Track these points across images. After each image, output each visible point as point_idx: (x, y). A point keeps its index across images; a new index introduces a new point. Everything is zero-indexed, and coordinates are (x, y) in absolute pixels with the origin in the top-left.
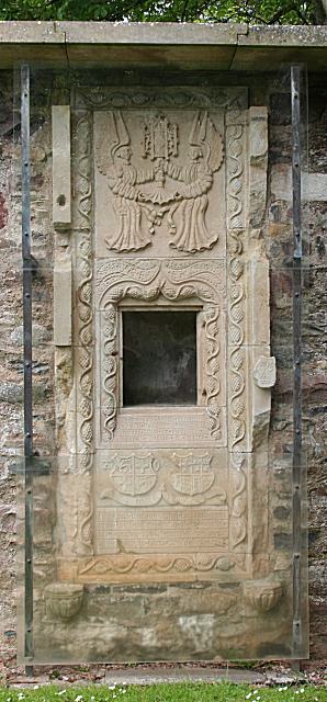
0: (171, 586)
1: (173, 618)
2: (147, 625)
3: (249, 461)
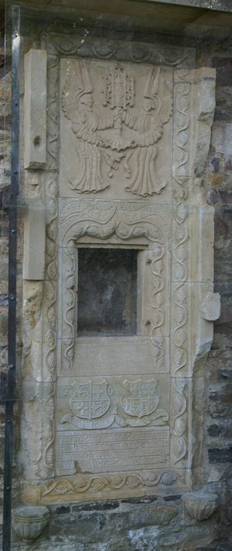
0: (123, 502)
1: (124, 532)
2: (101, 540)
3: (190, 386)
